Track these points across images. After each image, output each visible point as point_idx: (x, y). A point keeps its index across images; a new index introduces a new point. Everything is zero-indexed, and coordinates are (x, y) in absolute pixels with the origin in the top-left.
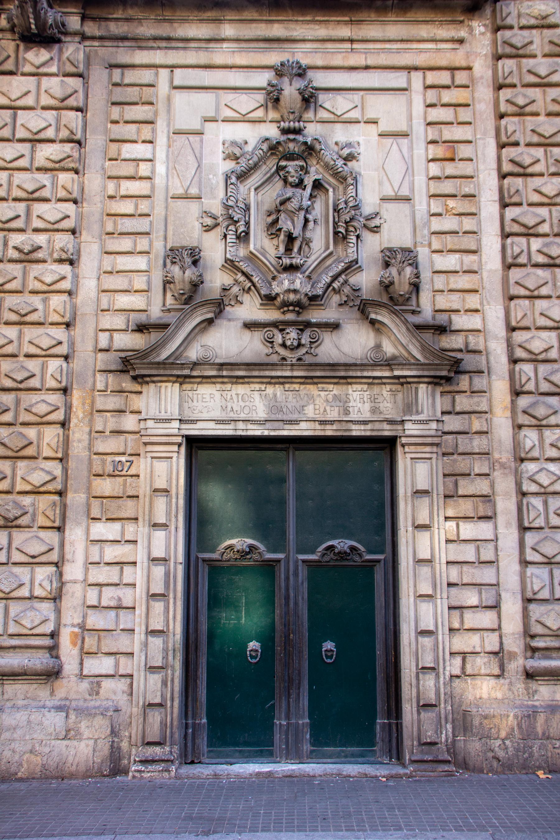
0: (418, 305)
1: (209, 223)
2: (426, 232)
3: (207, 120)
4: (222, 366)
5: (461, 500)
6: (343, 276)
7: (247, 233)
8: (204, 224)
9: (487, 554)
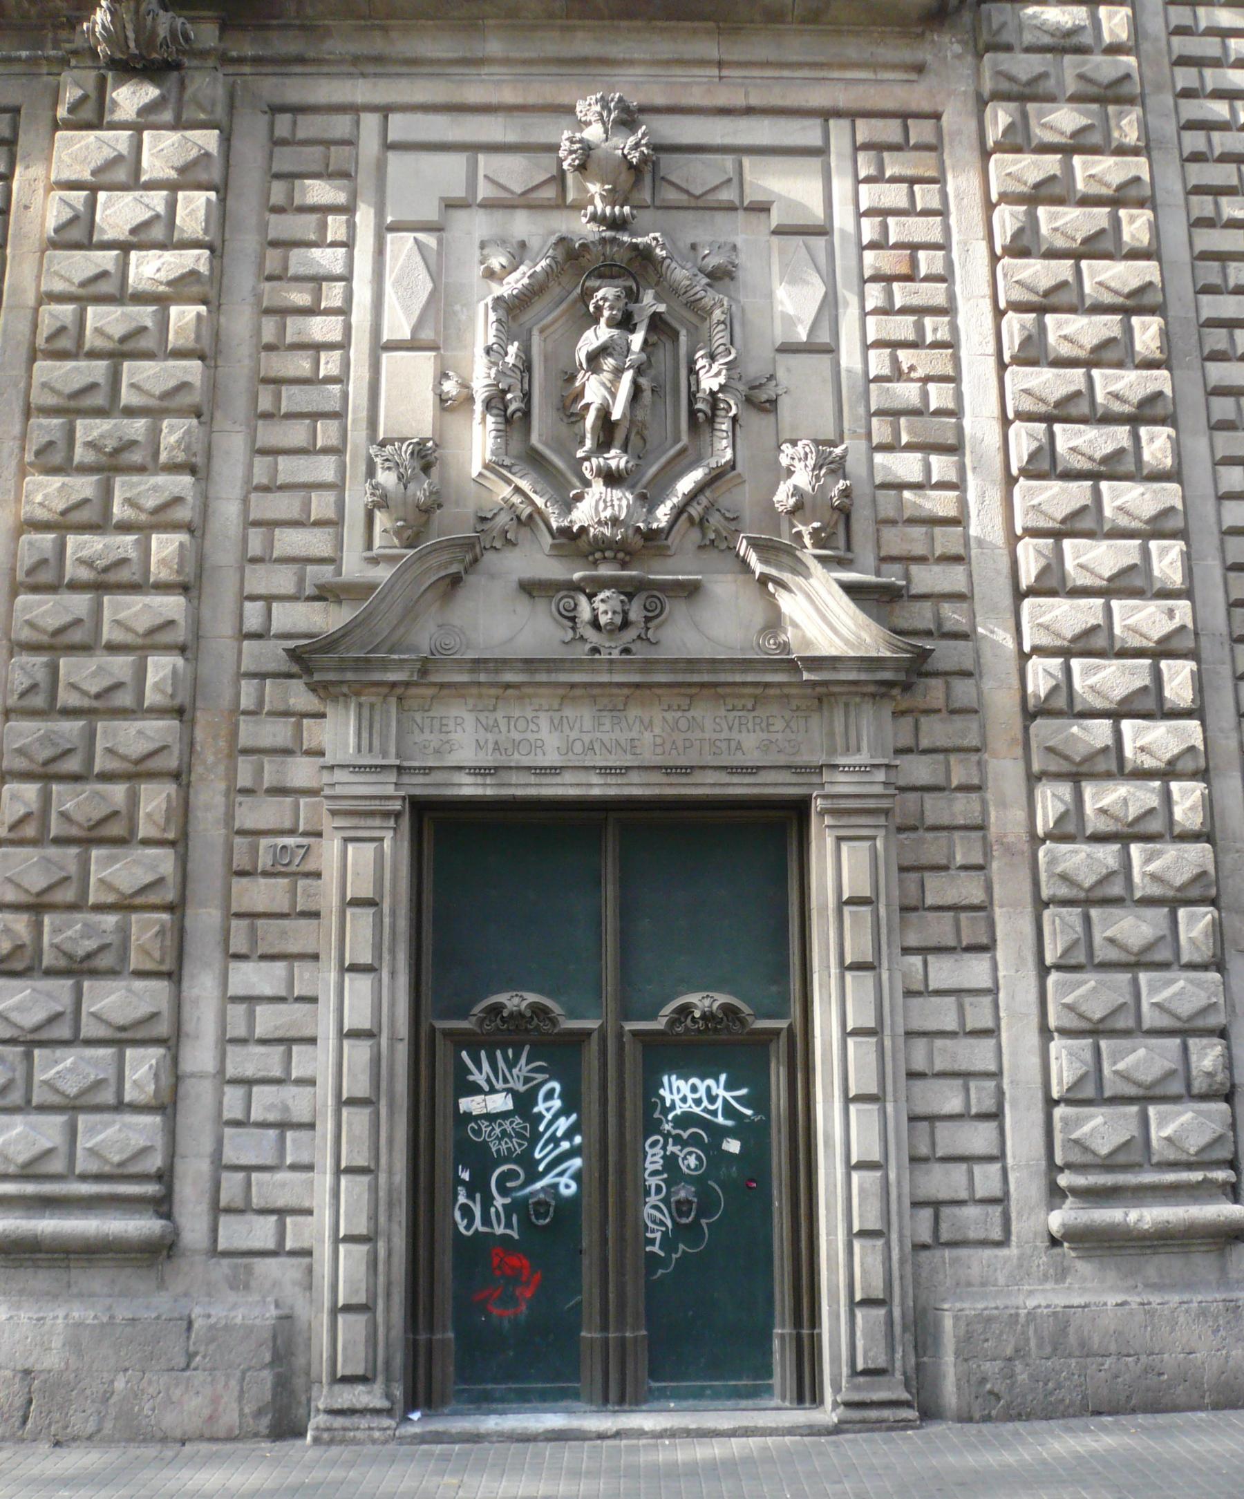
0: (849, 548)
2: (861, 411)
3: (451, 205)
4: (478, 664)
5: (931, 915)
6: (708, 493)
7: (527, 414)
9: (979, 1016)
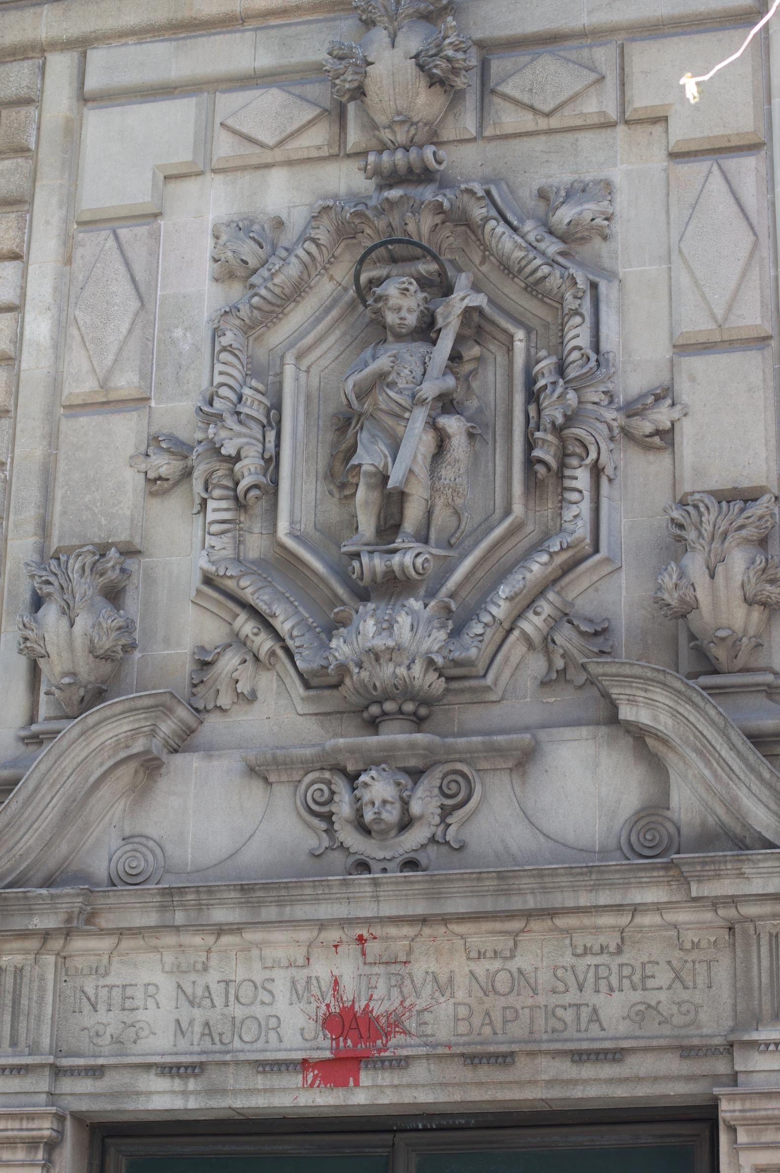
1: (164, 471)
7: (272, 490)
8: (151, 475)
